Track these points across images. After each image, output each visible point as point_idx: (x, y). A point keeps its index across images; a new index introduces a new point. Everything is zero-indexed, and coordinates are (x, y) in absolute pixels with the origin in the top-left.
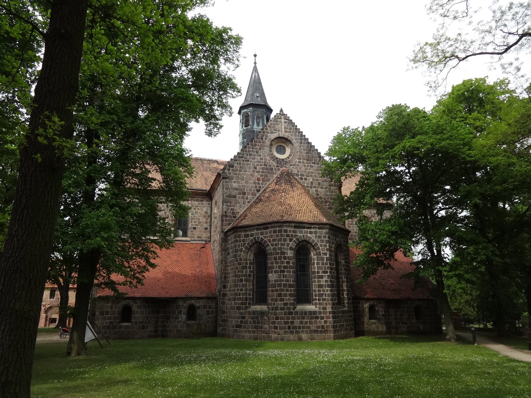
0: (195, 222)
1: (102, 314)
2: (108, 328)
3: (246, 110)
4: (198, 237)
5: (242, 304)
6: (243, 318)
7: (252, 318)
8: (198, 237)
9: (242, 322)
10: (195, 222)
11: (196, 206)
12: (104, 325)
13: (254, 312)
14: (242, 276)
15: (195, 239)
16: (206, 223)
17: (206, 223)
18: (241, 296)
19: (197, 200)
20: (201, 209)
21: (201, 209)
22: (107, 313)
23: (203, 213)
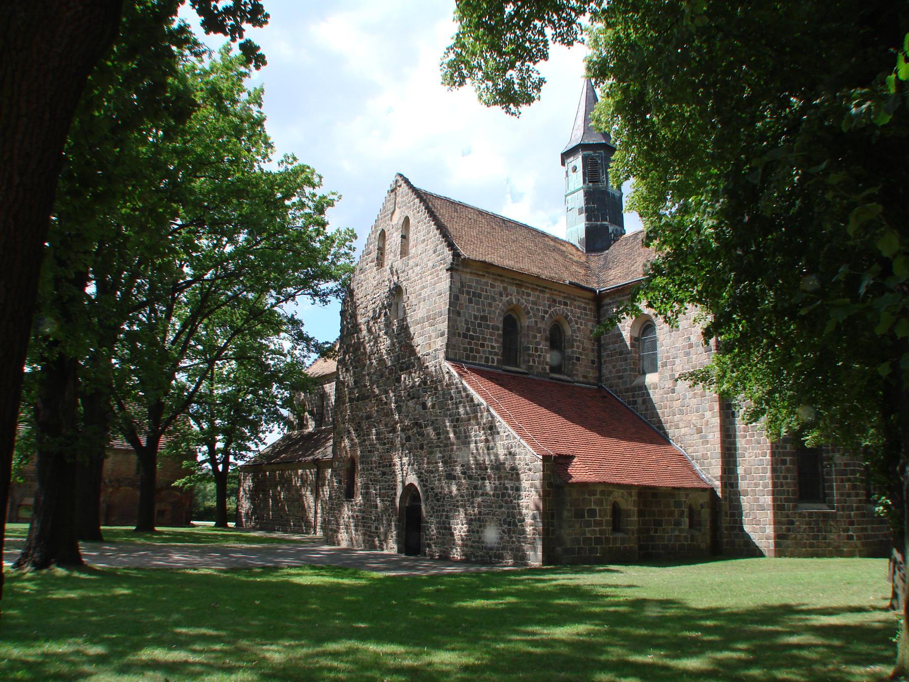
0: (578, 347)
1: (579, 514)
2: (598, 541)
3: (591, 152)
4: (584, 377)
5: (787, 500)
6: (791, 523)
7: (808, 523)
8: (584, 377)
9: (788, 530)
10: (578, 347)
11: (579, 318)
12: (588, 535)
13: (810, 515)
14: (784, 454)
15: (576, 379)
16: (593, 350)
17: (593, 350)
18: (785, 488)
19: (579, 307)
20: (586, 325)
21: (586, 325)
22: (592, 513)
23: (588, 332)
